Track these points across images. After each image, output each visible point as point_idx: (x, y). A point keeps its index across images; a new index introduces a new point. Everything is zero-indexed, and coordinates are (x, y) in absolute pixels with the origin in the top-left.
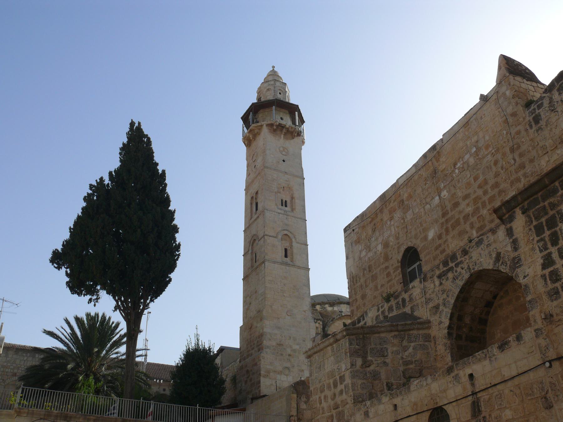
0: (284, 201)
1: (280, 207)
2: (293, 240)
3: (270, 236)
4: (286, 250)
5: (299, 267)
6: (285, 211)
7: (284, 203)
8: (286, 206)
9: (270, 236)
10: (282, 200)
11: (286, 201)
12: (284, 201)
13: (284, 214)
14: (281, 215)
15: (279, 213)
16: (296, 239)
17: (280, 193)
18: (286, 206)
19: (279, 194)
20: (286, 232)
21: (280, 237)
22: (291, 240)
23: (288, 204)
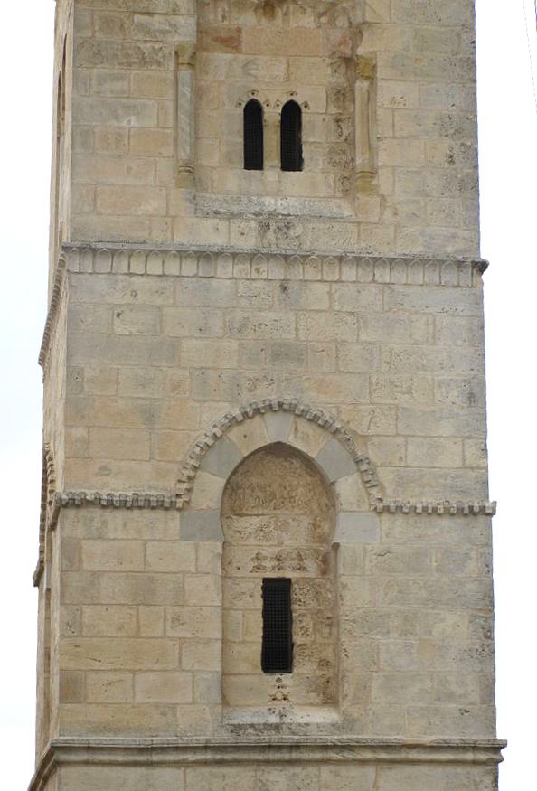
0: (272, 116)
1: (234, 178)
2: (347, 487)
3: (110, 505)
4: (277, 596)
5: (393, 754)
6: (266, 222)
7: (271, 137)
8: (292, 160)
9: (110, 505)
10: (253, 112)
11: (292, 114)
12: (272, 116)
13: (253, 256)
14: (225, 270)
15: (206, 256)
16: (370, 481)
17: (231, 42)
18: (292, 160)
19: (221, 59)
20: (270, 431)
21: (211, 487)
22: (326, 487)
23: (314, 136)
